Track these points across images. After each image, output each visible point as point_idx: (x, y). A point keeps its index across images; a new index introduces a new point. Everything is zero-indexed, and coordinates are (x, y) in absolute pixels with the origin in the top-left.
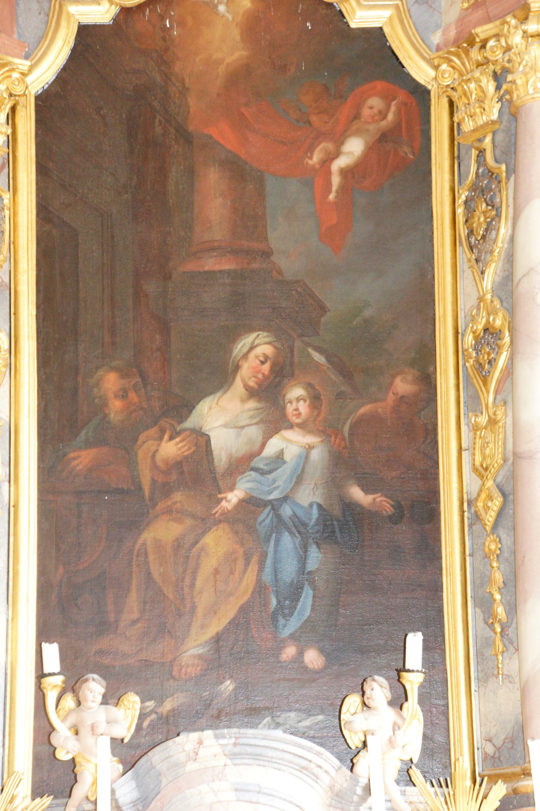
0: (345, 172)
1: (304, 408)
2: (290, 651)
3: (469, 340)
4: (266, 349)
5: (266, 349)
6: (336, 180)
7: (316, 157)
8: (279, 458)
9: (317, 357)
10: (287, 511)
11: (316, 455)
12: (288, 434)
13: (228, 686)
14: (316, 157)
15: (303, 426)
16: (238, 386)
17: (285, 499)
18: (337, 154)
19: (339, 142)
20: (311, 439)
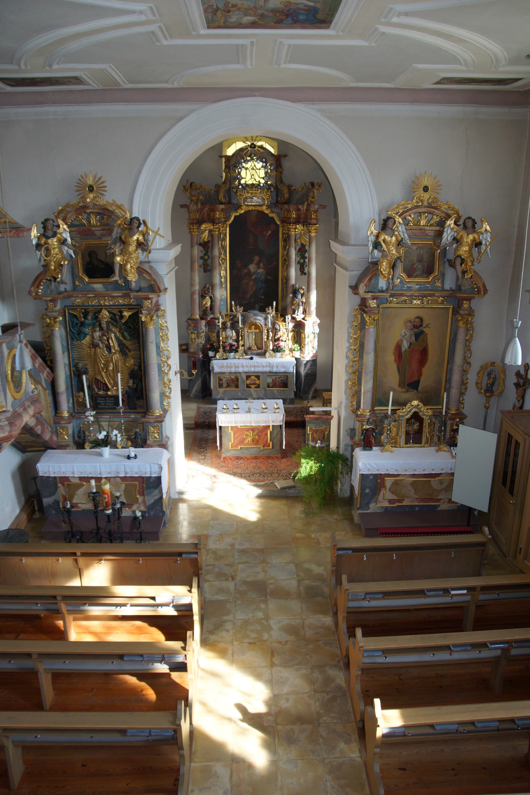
0: (268, 236)
1: (262, 266)
2: (260, 296)
3: (283, 259)
4: (258, 258)
5: (258, 258)
6: (267, 237)
7: (265, 233)
8: (259, 272)
9: (264, 260)
10: (260, 279)
11: (264, 272)
12: (261, 269)
13: (253, 300)
14: (265, 233)
15: (262, 268)
16: (254, 263)
17: (260, 278)
18: (267, 233)
19: (268, 231)
20: (263, 270)
